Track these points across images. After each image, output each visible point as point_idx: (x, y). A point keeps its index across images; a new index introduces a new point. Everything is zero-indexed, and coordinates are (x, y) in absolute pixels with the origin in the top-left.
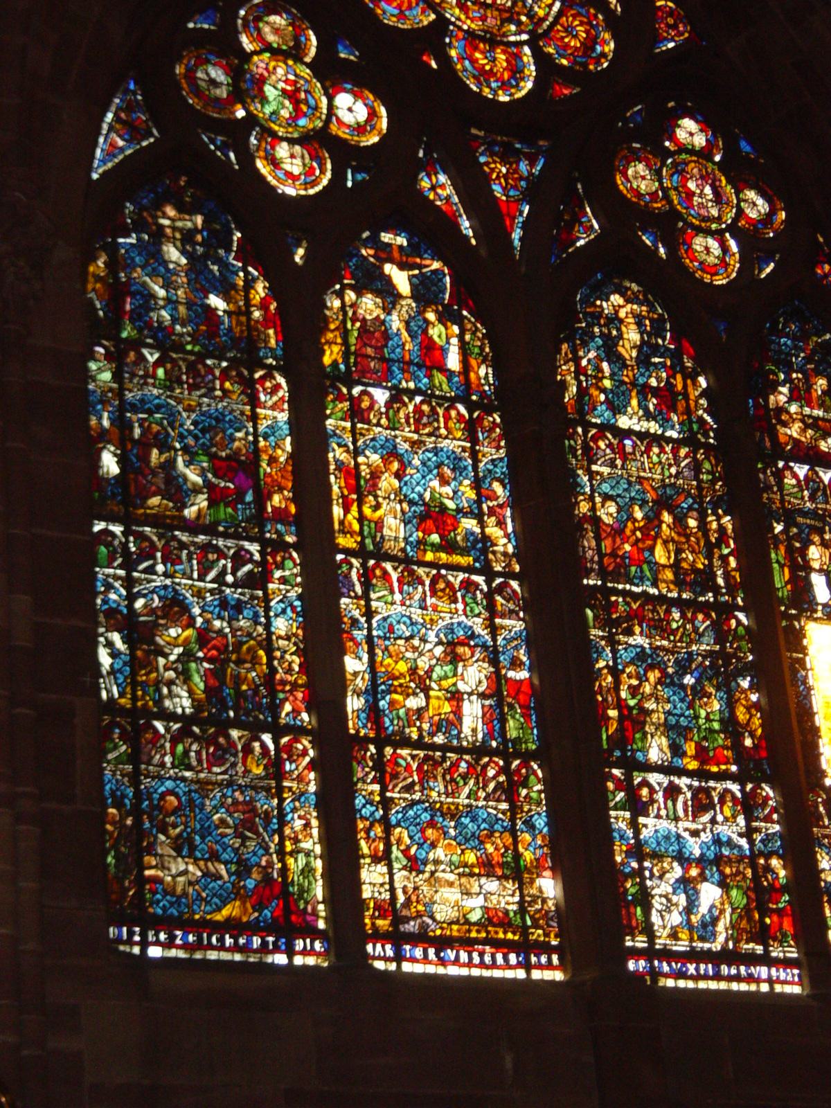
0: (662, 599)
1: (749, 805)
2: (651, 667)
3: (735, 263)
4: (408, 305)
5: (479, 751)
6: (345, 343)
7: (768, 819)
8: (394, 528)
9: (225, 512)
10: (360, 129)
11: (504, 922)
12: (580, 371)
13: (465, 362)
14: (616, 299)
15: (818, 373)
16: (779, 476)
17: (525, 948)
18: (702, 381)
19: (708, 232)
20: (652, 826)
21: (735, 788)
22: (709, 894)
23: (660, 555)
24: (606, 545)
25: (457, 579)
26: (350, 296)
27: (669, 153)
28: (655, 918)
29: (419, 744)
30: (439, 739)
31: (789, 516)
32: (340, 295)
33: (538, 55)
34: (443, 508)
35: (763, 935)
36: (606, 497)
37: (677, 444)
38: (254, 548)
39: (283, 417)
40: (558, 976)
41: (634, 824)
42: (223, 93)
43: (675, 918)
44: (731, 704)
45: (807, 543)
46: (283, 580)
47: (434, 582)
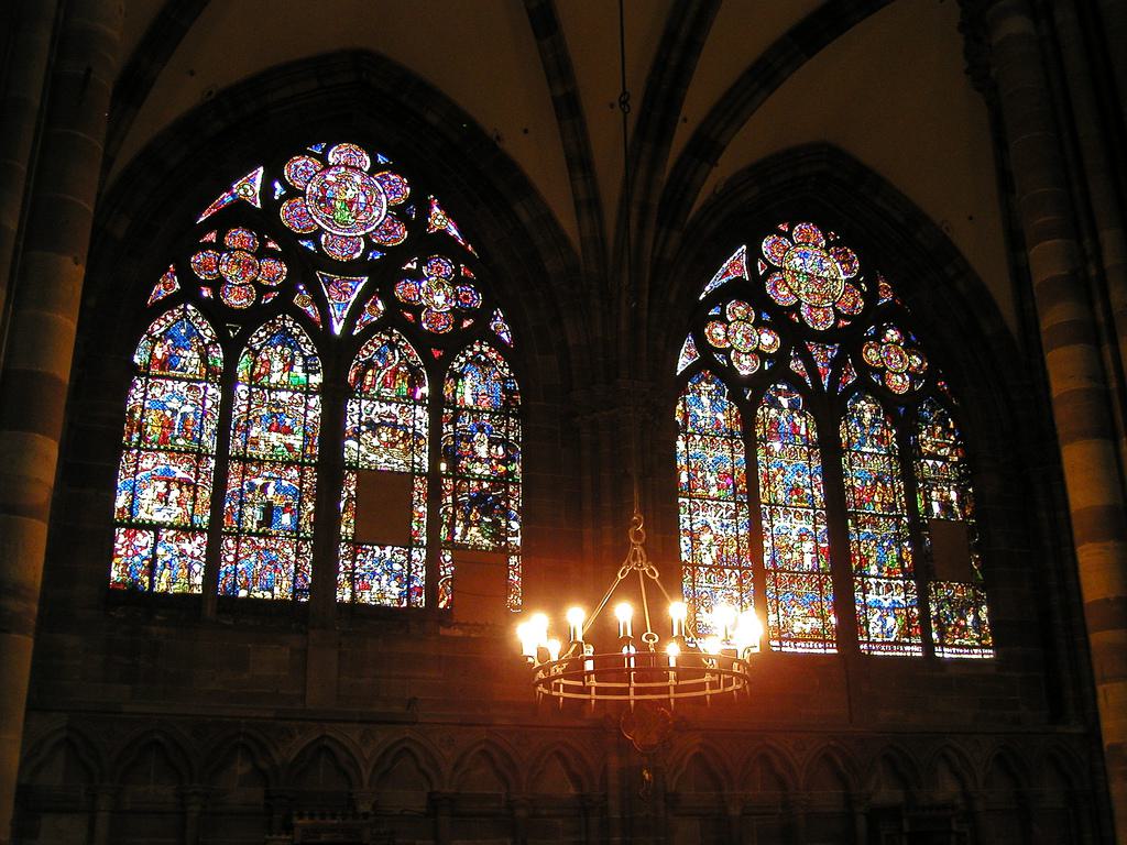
0: (877, 515)
1: (906, 589)
2: (871, 540)
3: (907, 385)
4: (786, 412)
5: (811, 573)
6: (765, 428)
7: (912, 593)
8: (781, 496)
9: (722, 493)
10: (770, 347)
11: (818, 634)
12: (849, 431)
13: (807, 431)
14: (863, 402)
15: (938, 424)
16: (922, 465)
17: (824, 641)
18: (894, 431)
19: (897, 374)
20: (871, 597)
21: (901, 582)
22: (890, 621)
23: (876, 498)
24: (857, 496)
25: (803, 511)
26: (766, 410)
27: (883, 344)
28: (870, 630)
29: (789, 572)
30: (796, 569)
31: (924, 481)
32: (762, 410)
33: (835, 310)
34: (799, 486)
35: (909, 635)
36: (857, 478)
37: (884, 456)
38: (733, 505)
39: (743, 457)
40: (835, 651)
41: (864, 597)
42: (721, 338)
43: (878, 630)
44: (901, 552)
45: (931, 490)
46: (743, 516)
47: (795, 512)
